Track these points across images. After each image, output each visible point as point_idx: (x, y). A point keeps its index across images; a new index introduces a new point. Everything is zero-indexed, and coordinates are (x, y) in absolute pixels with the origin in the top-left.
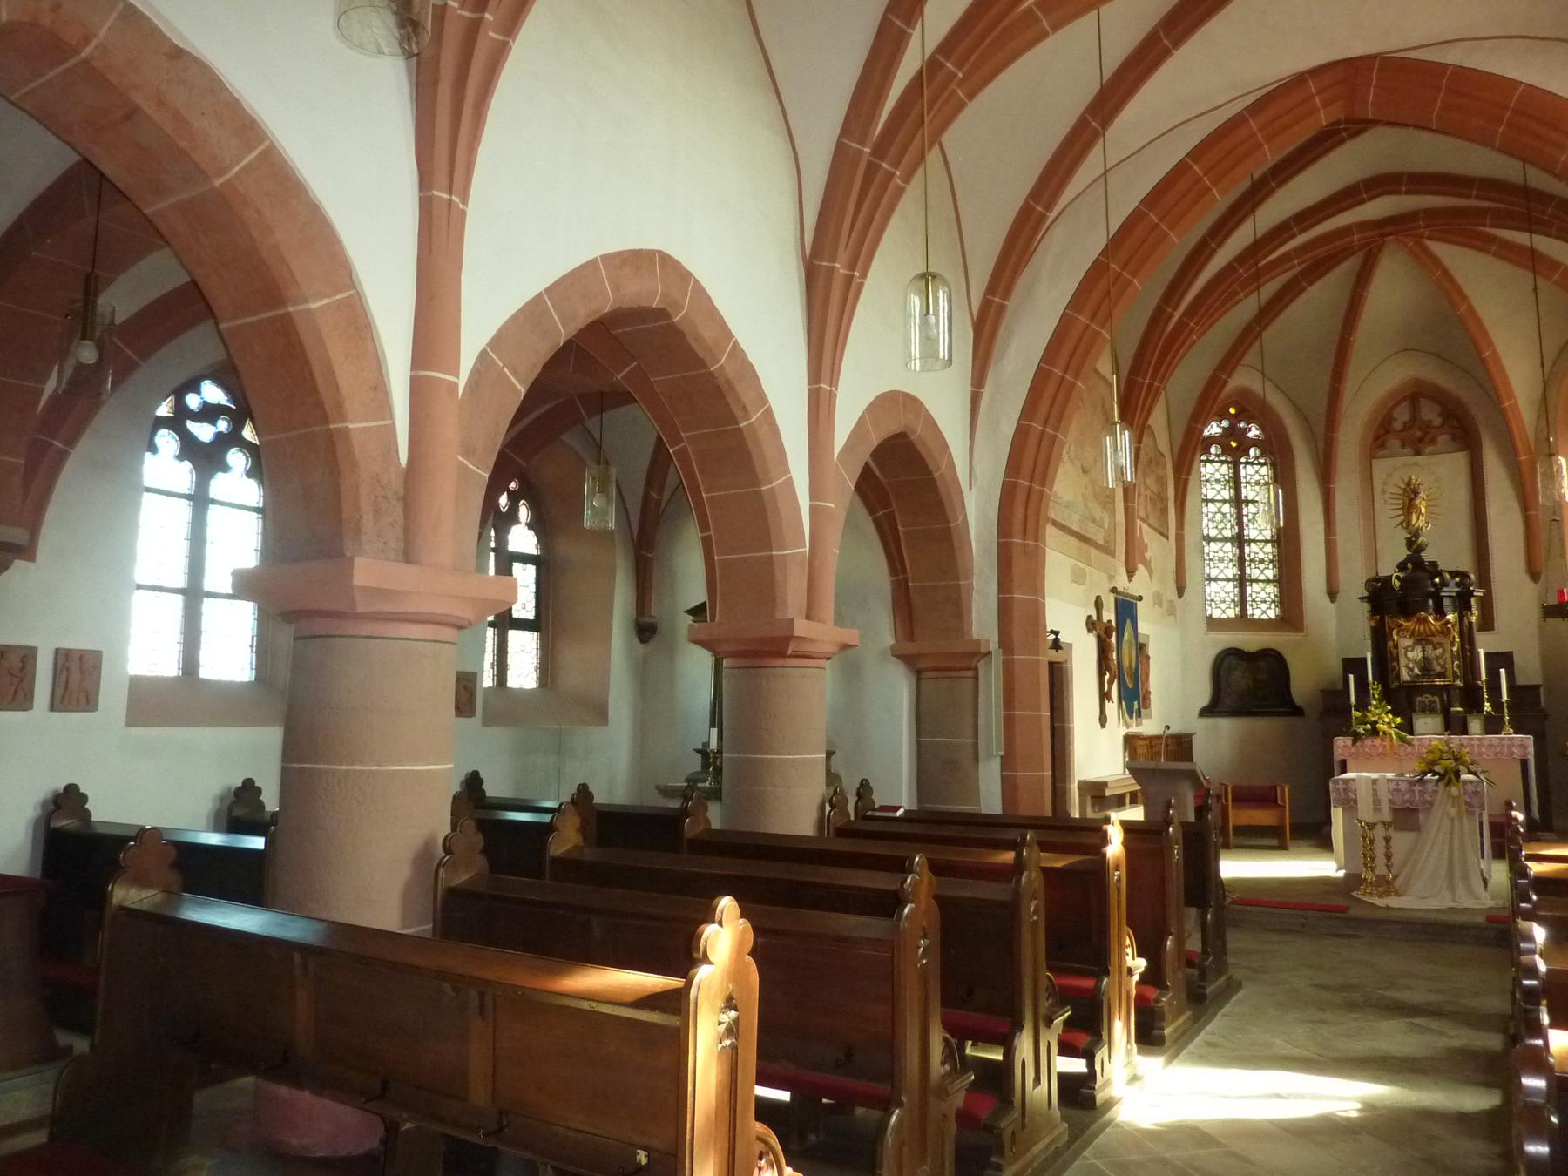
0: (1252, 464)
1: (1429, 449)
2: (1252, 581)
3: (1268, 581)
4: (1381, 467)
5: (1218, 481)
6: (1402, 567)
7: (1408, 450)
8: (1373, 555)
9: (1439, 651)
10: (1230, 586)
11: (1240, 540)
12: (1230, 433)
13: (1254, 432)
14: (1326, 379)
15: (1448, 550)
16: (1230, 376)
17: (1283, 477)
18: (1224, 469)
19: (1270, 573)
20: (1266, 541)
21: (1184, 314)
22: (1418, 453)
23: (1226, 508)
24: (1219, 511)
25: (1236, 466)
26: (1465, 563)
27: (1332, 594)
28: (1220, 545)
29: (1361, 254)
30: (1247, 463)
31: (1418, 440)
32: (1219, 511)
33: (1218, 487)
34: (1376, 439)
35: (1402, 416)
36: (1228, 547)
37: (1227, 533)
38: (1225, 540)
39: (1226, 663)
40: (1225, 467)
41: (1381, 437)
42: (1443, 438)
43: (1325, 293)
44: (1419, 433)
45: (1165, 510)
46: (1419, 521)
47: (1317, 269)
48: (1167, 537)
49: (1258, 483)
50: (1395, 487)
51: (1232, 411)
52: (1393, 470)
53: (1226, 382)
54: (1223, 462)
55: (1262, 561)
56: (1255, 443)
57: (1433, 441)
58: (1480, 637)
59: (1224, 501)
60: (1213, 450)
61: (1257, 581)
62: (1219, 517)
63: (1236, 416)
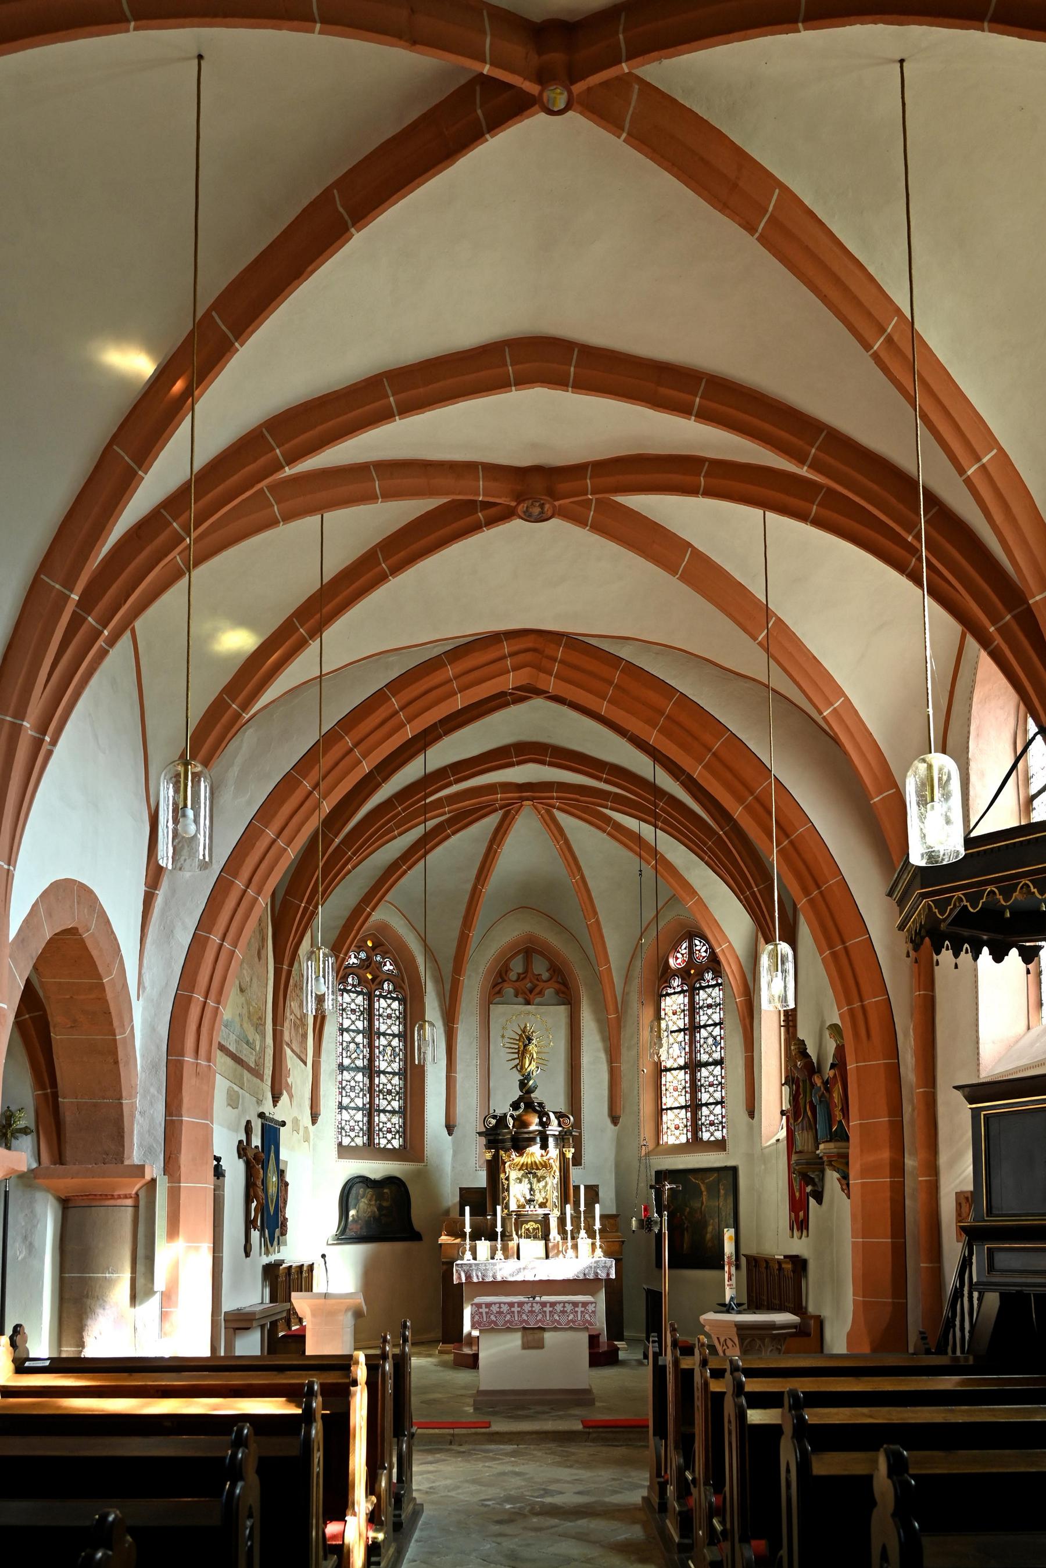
0: (385, 997)
1: (538, 1000)
2: (380, 1111)
3: (393, 1112)
4: (498, 1011)
5: (353, 1011)
6: (515, 1106)
7: (520, 999)
8: (486, 1093)
9: (542, 1183)
10: (359, 1116)
11: (371, 1071)
12: (366, 964)
13: (388, 967)
14: (458, 923)
15: (552, 1094)
16: (373, 909)
17: (412, 1017)
18: (360, 1000)
19: (395, 1105)
20: (394, 1074)
21: (341, 842)
22: (528, 1003)
23: (359, 1038)
24: (353, 1040)
25: (370, 998)
26: (562, 1108)
27: (450, 1128)
28: (352, 1074)
29: (501, 812)
30: (381, 996)
31: (528, 996)
32: (353, 1040)
33: (353, 1017)
34: (494, 986)
35: (517, 966)
36: (359, 1077)
37: (359, 1063)
38: (357, 1069)
39: (354, 1191)
40: (361, 998)
41: (498, 987)
42: (549, 992)
43: (466, 843)
44: (529, 985)
45: (305, 1036)
46: (531, 1067)
47: (461, 820)
48: (305, 1064)
49: (389, 1017)
50: (513, 1031)
51: (370, 944)
52: (510, 1017)
53: (370, 914)
54: (358, 993)
55: (389, 1092)
56: (390, 977)
57: (541, 993)
58: (574, 1171)
59: (358, 1032)
60: (350, 980)
61: (384, 1111)
62: (352, 1046)
63: (374, 948)
